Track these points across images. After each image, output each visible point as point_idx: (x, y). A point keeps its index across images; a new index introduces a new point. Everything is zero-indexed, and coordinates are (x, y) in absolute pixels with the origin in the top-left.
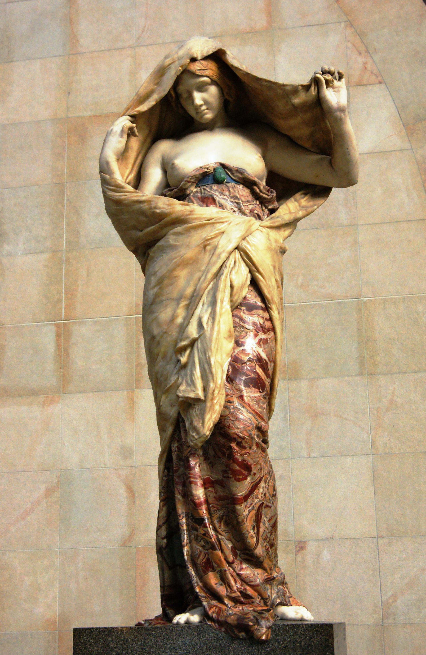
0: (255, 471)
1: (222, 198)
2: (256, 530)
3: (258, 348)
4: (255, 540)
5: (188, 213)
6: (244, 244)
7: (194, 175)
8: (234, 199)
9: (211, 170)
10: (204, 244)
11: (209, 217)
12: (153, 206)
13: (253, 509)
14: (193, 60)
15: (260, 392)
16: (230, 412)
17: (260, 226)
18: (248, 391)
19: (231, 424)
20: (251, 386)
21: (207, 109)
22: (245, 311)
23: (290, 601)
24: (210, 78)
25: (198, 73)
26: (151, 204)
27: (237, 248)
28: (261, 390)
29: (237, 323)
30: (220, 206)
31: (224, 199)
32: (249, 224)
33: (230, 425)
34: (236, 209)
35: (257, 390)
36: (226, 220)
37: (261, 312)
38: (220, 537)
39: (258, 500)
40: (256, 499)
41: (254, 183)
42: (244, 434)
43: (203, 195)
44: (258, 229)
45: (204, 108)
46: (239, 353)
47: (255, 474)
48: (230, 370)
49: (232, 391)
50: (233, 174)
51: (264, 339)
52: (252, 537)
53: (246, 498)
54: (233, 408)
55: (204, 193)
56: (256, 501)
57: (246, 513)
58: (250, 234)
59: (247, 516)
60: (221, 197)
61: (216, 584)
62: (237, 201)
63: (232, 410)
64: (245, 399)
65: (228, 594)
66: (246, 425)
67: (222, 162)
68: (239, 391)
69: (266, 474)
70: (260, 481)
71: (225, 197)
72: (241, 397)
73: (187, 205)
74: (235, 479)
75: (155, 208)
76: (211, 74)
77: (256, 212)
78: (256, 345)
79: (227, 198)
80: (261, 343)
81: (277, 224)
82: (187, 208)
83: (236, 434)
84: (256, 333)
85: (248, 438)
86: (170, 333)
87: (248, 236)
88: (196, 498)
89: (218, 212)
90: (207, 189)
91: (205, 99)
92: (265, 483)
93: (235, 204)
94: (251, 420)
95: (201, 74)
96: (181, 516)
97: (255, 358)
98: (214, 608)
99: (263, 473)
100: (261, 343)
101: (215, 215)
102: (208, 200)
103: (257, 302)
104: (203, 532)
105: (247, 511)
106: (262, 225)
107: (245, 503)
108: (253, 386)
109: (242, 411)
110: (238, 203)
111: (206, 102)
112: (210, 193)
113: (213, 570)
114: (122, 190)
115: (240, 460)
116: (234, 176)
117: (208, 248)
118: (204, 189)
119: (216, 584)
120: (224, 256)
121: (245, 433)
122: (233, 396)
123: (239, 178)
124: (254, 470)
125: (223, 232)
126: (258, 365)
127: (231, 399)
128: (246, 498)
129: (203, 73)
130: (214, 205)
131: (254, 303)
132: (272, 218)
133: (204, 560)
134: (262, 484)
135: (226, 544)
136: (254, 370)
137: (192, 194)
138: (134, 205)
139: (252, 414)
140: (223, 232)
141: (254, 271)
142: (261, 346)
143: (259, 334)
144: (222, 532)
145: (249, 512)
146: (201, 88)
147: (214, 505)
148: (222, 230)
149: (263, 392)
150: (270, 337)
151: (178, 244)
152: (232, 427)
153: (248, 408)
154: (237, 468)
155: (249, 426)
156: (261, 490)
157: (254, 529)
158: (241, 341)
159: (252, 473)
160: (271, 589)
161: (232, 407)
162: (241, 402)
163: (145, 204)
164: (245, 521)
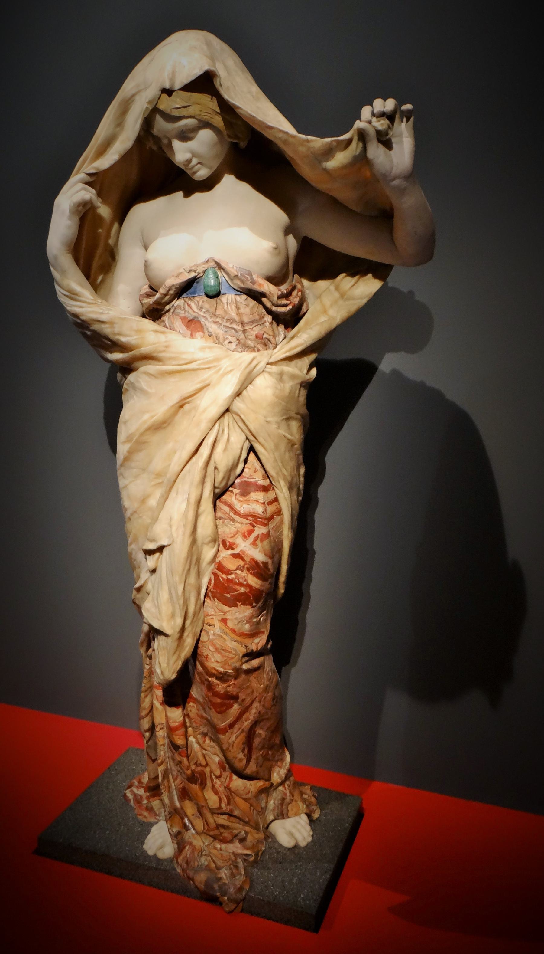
0: (244, 697)
1: (213, 322)
2: (246, 751)
3: (253, 549)
4: (245, 761)
5: (162, 349)
6: (238, 405)
7: (173, 285)
8: (231, 323)
9: (199, 274)
10: (181, 403)
11: (189, 357)
12: (116, 330)
13: (243, 731)
14: (168, 92)
15: (253, 607)
16: (209, 638)
17: (268, 364)
18: (233, 612)
19: (210, 656)
20: (239, 604)
21: (199, 163)
22: (238, 496)
23: (288, 811)
24: (197, 119)
25: (176, 113)
26: (114, 327)
27: (228, 410)
28: (254, 604)
29: (227, 513)
30: (210, 336)
31: (216, 322)
32: (248, 370)
33: (207, 655)
34: (233, 339)
35: (248, 607)
36: (215, 364)
37: (260, 496)
38: (204, 752)
39: (250, 721)
40: (246, 721)
41: (263, 295)
42: (226, 669)
43: (187, 314)
44: (263, 371)
45: (194, 161)
46: (225, 559)
47: (243, 700)
48: (213, 582)
49: (213, 610)
50: (232, 280)
51: (263, 534)
52: (241, 760)
53: (231, 726)
54: (214, 634)
55: (188, 313)
56: (246, 723)
57: (233, 738)
58: (250, 383)
59: (234, 742)
60: (213, 319)
61: (193, 815)
62: (235, 326)
63: (211, 637)
64: (230, 624)
65: (205, 831)
66: (228, 657)
68: (222, 612)
69: (260, 694)
70: (252, 703)
71: (218, 320)
72: (224, 621)
73: (163, 333)
74: (216, 711)
75: (119, 334)
76: (197, 113)
77: (265, 336)
78: (251, 547)
79: (221, 322)
80: (258, 542)
81: (298, 350)
82: (162, 338)
83: (215, 669)
84: (252, 528)
85: (230, 671)
86: (140, 515)
87: (246, 388)
88: (171, 721)
89: (202, 349)
90: (193, 306)
91: (194, 151)
92: (260, 701)
93: (233, 331)
94: (236, 650)
95: (181, 115)
96: (159, 727)
97: (247, 566)
98: (187, 847)
99: (255, 694)
100: (258, 542)
101: (200, 355)
102: (193, 324)
103: (257, 479)
104: (179, 760)
105: (234, 737)
106: (271, 360)
107: (231, 730)
108: (242, 604)
109: (224, 639)
110: (235, 330)
111: (194, 155)
112: (196, 315)
113: (190, 799)
115: (222, 692)
116: (233, 283)
117: (187, 407)
118: (189, 305)
119: (193, 815)
120: (204, 425)
121: (227, 667)
122: (214, 617)
123: (241, 288)
124: (242, 696)
125: (208, 385)
126: (251, 574)
127: (211, 622)
128: (231, 726)
129: (184, 112)
130: (201, 333)
131: (253, 481)
132: (292, 338)
133: (181, 786)
134: (256, 704)
135: (212, 759)
136: (245, 583)
137: (172, 310)
138: (94, 324)
139: (238, 642)
140: (208, 385)
141: (253, 441)
142: (257, 546)
143: (255, 528)
144: (206, 748)
145: (237, 737)
146: (185, 136)
147: (197, 721)
148: (207, 382)
149: (257, 603)
150: (274, 524)
151: (150, 390)
152: (211, 659)
153: (233, 635)
154: (219, 701)
155: (232, 658)
156: (253, 711)
157: (243, 751)
158: (229, 542)
159: (240, 700)
160: (267, 797)
161: (212, 632)
162: (223, 627)
163: (107, 326)
164: (230, 748)
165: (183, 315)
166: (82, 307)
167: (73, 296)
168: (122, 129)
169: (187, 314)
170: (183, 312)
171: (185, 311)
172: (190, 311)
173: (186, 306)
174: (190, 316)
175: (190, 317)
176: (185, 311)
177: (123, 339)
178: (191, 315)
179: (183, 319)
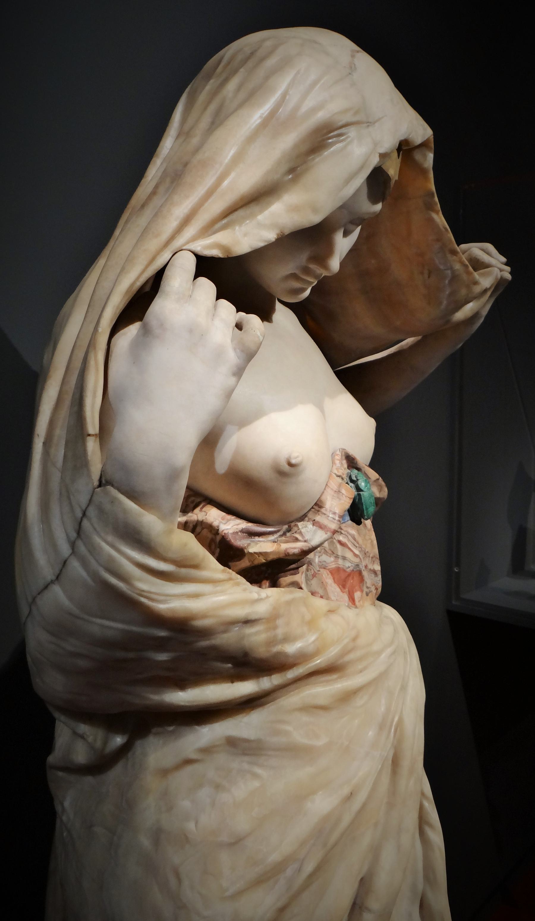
12: (280, 632)
67: (353, 452)
112: (357, 560)
114: (193, 572)
138: (225, 632)
165: (333, 566)
166: (196, 596)
167: (183, 571)
168: (295, 181)
169: (340, 562)
170: (332, 559)
171: (337, 557)
172: (349, 555)
173: (338, 546)
174: (348, 564)
175: (348, 565)
176: (337, 557)
177: (291, 649)
178: (350, 562)
179: (336, 572)
